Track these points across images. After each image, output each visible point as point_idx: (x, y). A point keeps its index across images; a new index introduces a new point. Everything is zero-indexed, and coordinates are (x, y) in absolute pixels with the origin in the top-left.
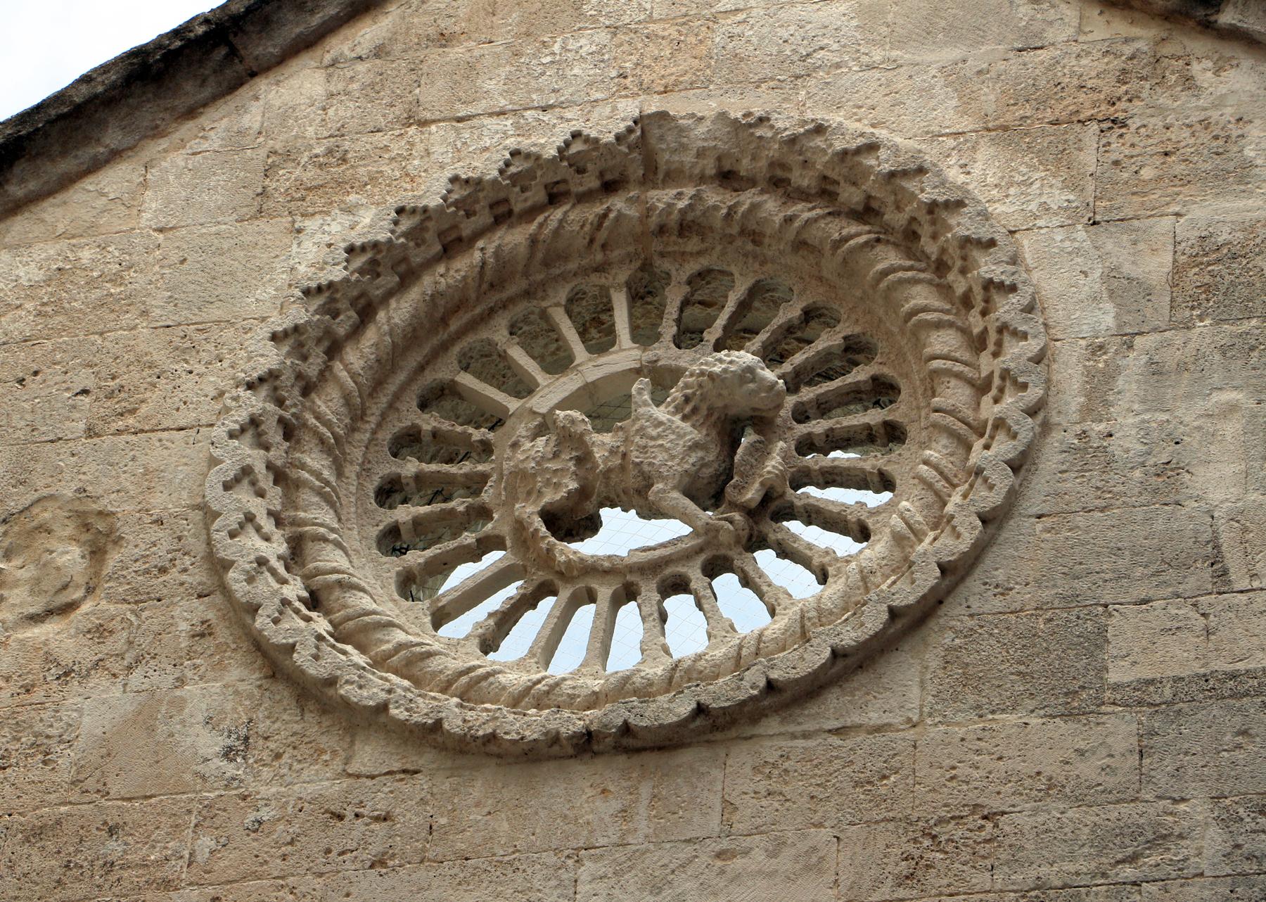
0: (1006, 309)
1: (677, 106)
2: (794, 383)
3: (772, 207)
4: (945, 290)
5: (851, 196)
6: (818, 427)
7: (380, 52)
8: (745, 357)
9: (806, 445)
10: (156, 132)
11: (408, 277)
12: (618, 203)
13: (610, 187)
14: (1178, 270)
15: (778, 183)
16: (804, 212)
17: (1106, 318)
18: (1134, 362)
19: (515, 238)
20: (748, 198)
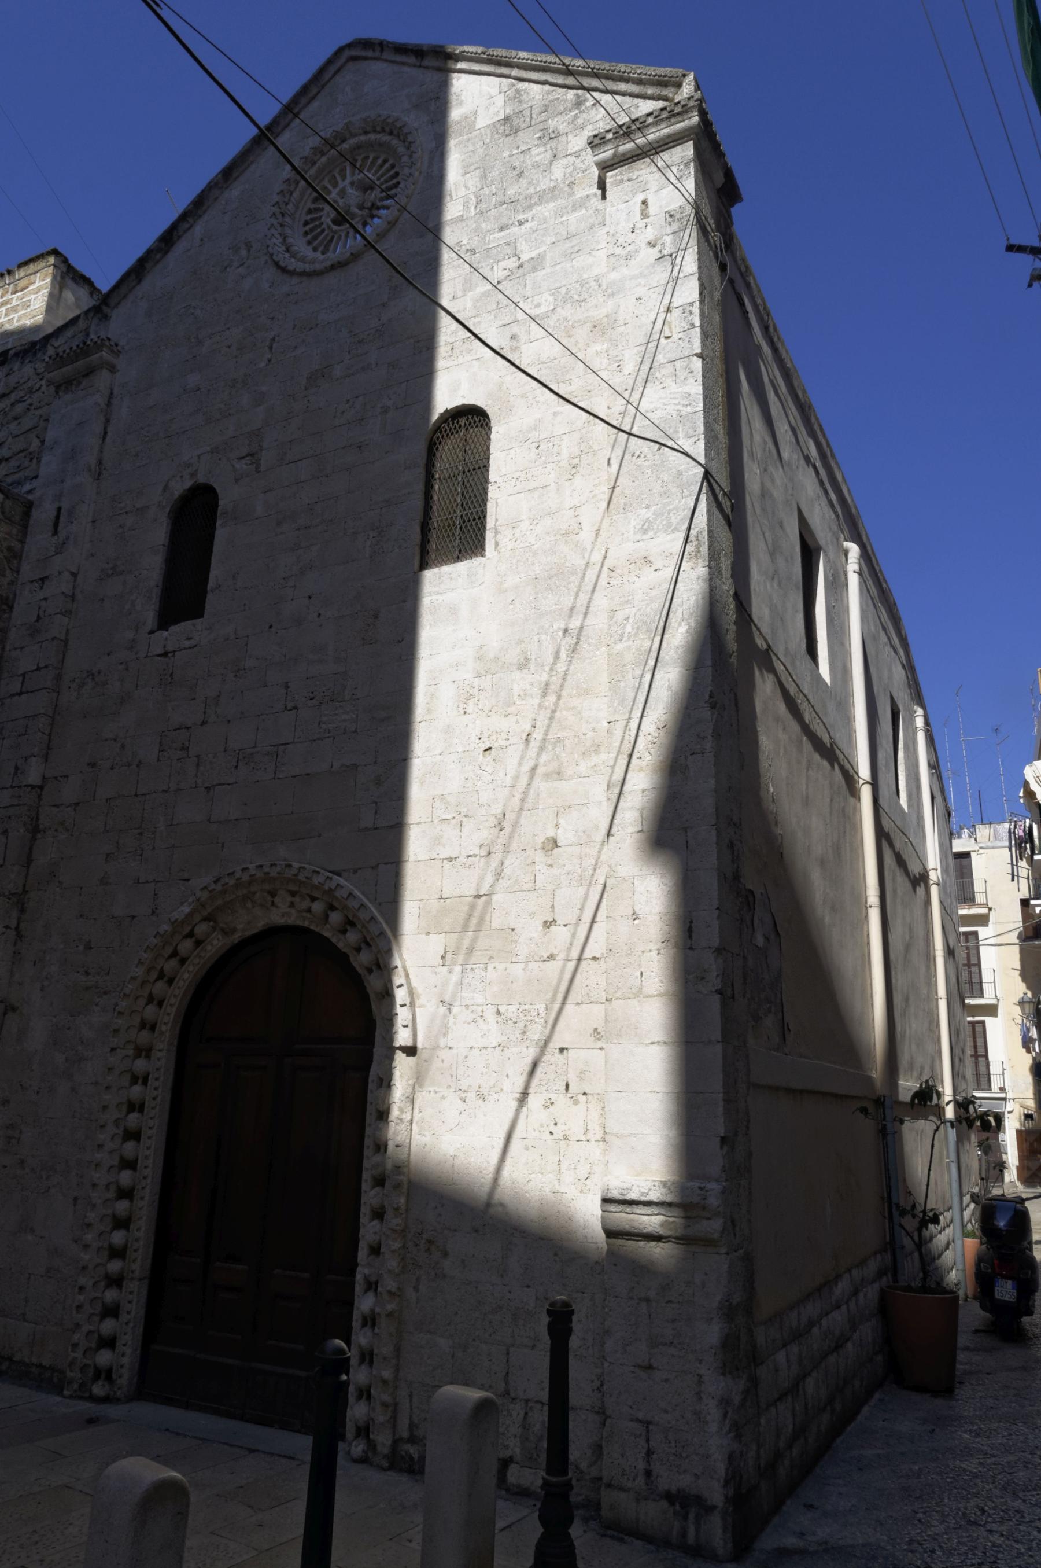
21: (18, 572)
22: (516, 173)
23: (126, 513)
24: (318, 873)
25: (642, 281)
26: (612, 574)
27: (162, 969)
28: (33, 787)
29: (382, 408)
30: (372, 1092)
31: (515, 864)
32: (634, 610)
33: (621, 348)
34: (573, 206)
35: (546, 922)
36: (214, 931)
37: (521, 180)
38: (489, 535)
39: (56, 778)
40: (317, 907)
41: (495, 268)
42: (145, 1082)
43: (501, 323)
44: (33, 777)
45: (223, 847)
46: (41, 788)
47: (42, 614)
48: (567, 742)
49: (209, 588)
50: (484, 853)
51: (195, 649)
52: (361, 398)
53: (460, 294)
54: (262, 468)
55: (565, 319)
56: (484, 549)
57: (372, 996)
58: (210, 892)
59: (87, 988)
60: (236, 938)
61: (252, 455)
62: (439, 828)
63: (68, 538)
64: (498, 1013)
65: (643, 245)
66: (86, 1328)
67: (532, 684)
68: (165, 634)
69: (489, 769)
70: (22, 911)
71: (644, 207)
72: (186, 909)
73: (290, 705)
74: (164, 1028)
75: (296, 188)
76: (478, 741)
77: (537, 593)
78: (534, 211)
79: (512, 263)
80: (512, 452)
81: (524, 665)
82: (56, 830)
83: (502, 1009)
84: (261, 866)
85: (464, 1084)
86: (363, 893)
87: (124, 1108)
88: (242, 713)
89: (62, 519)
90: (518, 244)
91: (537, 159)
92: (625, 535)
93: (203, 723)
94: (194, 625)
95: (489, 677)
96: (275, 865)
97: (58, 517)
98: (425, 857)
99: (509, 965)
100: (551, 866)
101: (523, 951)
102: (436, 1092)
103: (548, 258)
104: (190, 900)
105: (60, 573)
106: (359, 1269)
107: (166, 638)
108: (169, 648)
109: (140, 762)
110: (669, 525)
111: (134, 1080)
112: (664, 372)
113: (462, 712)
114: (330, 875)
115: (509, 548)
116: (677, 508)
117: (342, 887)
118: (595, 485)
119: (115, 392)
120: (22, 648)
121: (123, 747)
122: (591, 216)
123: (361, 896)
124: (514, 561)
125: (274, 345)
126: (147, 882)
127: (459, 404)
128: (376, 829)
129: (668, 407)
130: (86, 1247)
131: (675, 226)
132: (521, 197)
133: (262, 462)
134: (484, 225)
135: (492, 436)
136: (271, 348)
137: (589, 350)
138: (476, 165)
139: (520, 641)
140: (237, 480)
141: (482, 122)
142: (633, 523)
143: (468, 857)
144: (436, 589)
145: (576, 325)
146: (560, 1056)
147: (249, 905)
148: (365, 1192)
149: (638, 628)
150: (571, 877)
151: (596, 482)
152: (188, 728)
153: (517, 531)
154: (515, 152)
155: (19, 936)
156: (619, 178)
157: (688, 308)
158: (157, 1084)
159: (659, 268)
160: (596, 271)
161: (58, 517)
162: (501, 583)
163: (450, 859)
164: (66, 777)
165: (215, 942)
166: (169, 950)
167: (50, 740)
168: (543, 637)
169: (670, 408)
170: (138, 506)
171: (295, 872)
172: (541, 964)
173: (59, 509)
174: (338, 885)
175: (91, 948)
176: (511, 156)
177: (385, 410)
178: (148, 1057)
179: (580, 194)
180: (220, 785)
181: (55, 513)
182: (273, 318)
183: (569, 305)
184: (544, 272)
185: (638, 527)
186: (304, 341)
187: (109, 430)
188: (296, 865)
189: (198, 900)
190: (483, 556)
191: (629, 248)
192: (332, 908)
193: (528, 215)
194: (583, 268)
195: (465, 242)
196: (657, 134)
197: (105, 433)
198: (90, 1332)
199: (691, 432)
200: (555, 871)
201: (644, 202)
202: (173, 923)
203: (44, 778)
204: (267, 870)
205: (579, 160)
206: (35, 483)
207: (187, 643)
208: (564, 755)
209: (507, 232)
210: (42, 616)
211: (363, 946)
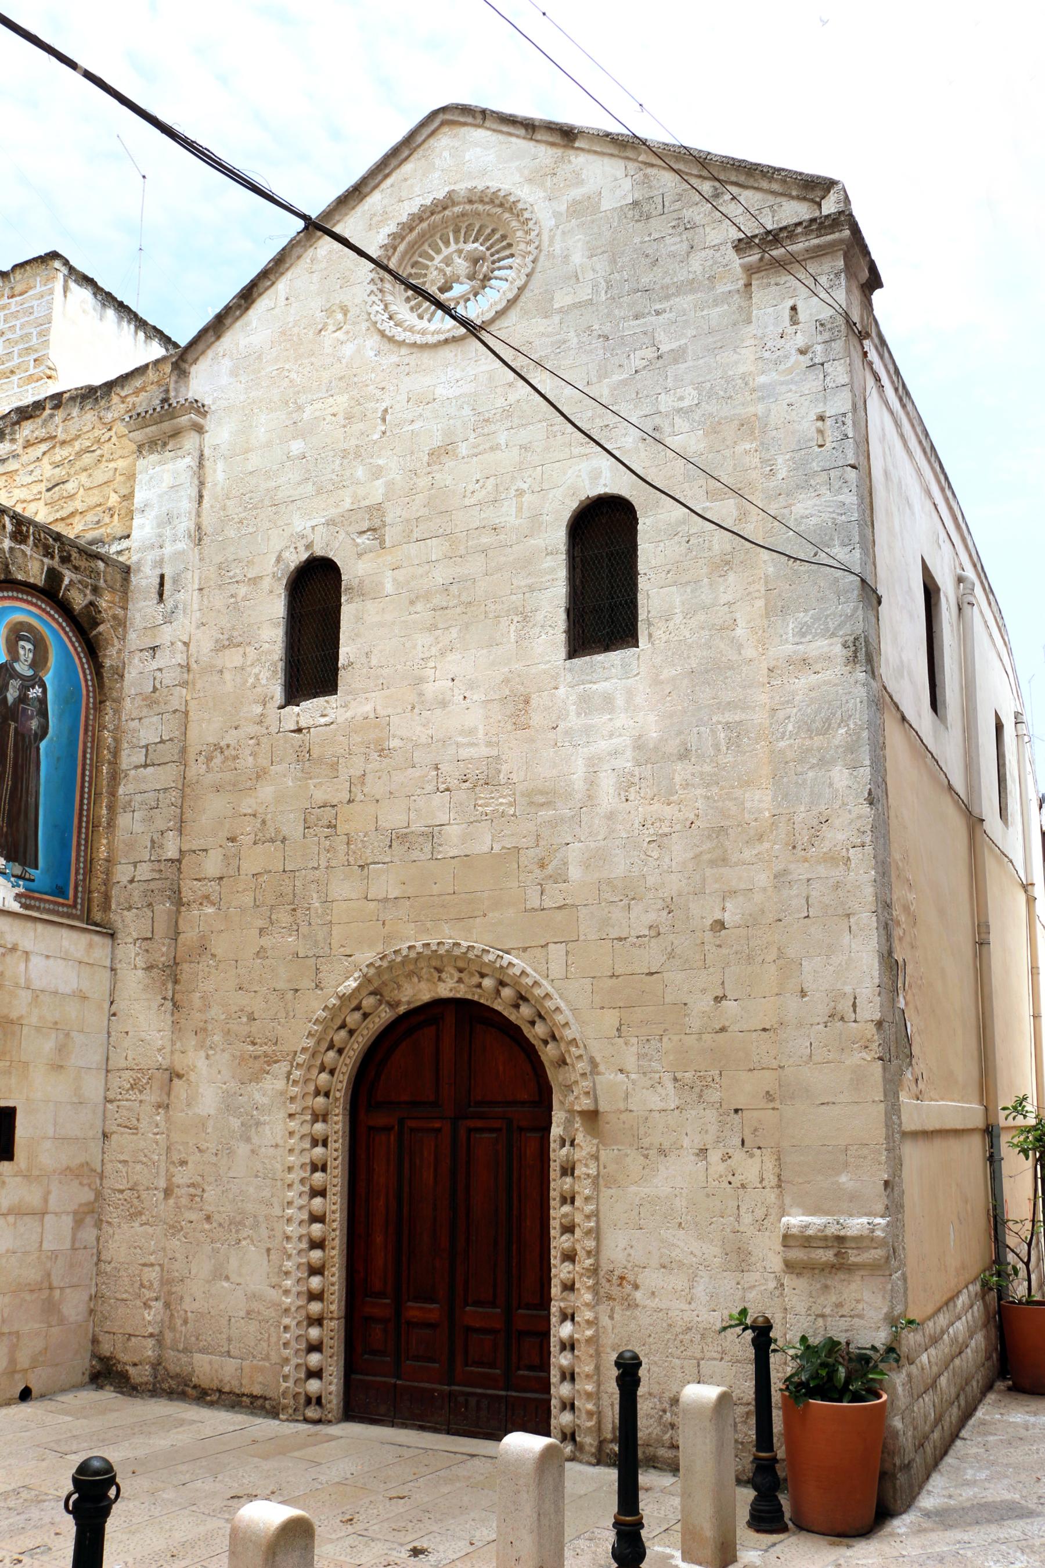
0: (531, 224)
1: (456, 187)
2: (488, 249)
3: (480, 207)
4: (519, 221)
5: (497, 202)
6: (496, 257)
7: (392, 186)
8: (476, 245)
9: (493, 262)
10: (346, 214)
11: (403, 239)
12: (447, 212)
13: (445, 209)
14: (568, 208)
15: (482, 201)
16: (487, 207)
17: (553, 222)
18: (559, 232)
19: (424, 225)
20: (475, 206)
21: (124, 639)
22: (649, 260)
23: (237, 582)
24: (488, 951)
25: (794, 388)
26: (772, 674)
27: (332, 1040)
28: (172, 861)
29: (517, 490)
30: (554, 1151)
31: (686, 944)
32: (795, 710)
33: (773, 452)
34: (714, 301)
35: (716, 998)
36: (380, 1004)
37: (655, 268)
38: (642, 627)
39: (194, 851)
40: (488, 983)
41: (632, 356)
42: (325, 1144)
43: (642, 413)
44: (172, 853)
45: (384, 924)
46: (179, 861)
47: (158, 686)
48: (730, 831)
49: (340, 665)
50: (653, 933)
51: (332, 726)
52: (492, 478)
53: (594, 380)
54: (388, 544)
55: (711, 415)
56: (637, 641)
57: (547, 1064)
58: (377, 968)
59: (256, 1058)
60: (402, 1009)
61: (374, 530)
62: (606, 910)
63: (176, 607)
64: (676, 1080)
65: (793, 352)
67: (693, 775)
68: (296, 709)
69: (655, 854)
70: (176, 982)
71: (793, 313)
72: (352, 984)
73: (442, 787)
74: (338, 1095)
75: (394, 253)
76: (641, 828)
77: (694, 686)
78: (672, 302)
79: (650, 353)
80: (662, 544)
81: (684, 755)
82: (201, 904)
83: (679, 1075)
85: (646, 1142)
86: (535, 970)
88: (391, 793)
89: (167, 587)
90: (656, 335)
91: (673, 248)
92: (784, 637)
93: (349, 801)
94: (327, 702)
95: (649, 766)
96: (443, 943)
97: (162, 584)
98: (592, 937)
99: (683, 1036)
100: (720, 946)
101: (696, 1024)
102: (619, 1150)
103: (690, 351)
104: (356, 975)
105: (172, 644)
106: (553, 1303)
107: (298, 714)
108: (303, 724)
109: (284, 838)
110: (827, 629)
112: (819, 480)
113: (624, 799)
114: (501, 953)
115: (664, 640)
116: (834, 614)
117: (514, 965)
118: (749, 583)
119: (207, 452)
120: (140, 719)
121: (264, 822)
122: (734, 313)
123: (535, 974)
124: (670, 653)
125: (388, 417)
126: (307, 957)
127: (602, 492)
128: (543, 909)
129: (823, 515)
131: (826, 336)
132: (657, 287)
133: (387, 538)
134: (616, 312)
135: (639, 527)
136: (384, 420)
137: (737, 447)
138: (603, 249)
139: (680, 733)
140: (360, 555)
141: (606, 205)
142: (791, 626)
143: (638, 937)
144: (589, 678)
145: (723, 421)
146: (735, 1116)
147: (415, 980)
148: (555, 1238)
149: (799, 727)
150: (739, 956)
151: (750, 580)
152: (333, 806)
153: (671, 624)
154: (647, 239)
155: (175, 1005)
156: (765, 281)
157: (841, 419)
158: (337, 1145)
159: (811, 376)
160: (742, 369)
161: (162, 584)
162: (657, 675)
163: (620, 939)
164: (206, 850)
165: (383, 1015)
166: (339, 1022)
167: (182, 813)
168: (703, 729)
169: (825, 516)
170: (249, 576)
171: (464, 950)
172: (713, 1035)
173: (162, 577)
174: (510, 963)
175: (255, 1019)
176: (642, 243)
177: (520, 493)
178: (325, 1121)
179: (722, 288)
180: (375, 863)
181: (158, 580)
182: (383, 389)
183: (715, 401)
184: (685, 365)
185: (796, 630)
186: (421, 415)
187: (205, 493)
188: (465, 944)
189: (365, 976)
190: (638, 647)
191: (778, 353)
192: (502, 983)
193: (665, 305)
194: (728, 365)
195: (596, 327)
196: (807, 244)
197: (201, 497)
199: (846, 541)
200: (724, 951)
201: (794, 308)
203: (181, 851)
204: (434, 948)
205: (718, 254)
206: (125, 544)
207: (323, 720)
208: (727, 843)
209: (642, 321)
210: (159, 687)
211: (537, 1019)
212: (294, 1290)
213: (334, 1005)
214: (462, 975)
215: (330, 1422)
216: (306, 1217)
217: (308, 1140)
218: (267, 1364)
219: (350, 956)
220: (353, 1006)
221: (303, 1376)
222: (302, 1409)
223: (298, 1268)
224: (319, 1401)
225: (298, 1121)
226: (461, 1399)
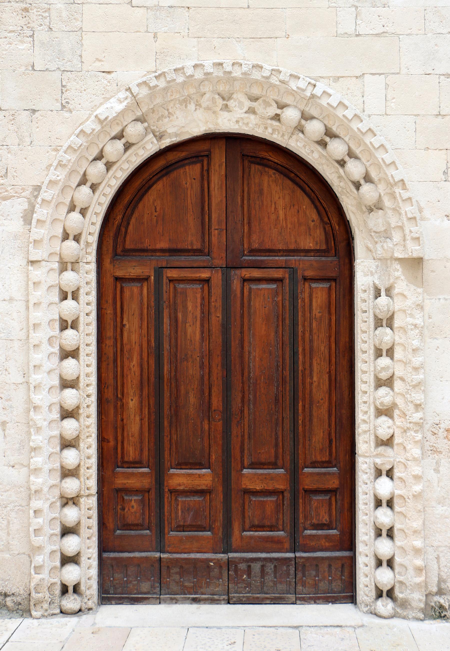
66: (49, 548)
84: (221, 64)
87: (57, 325)
111: (64, 296)
130: (36, 471)
166: (95, 152)
198: (53, 552)
202: (101, 122)
212: (46, 467)
213: (93, 130)
214: (254, 104)
215: (90, 609)
216: (56, 382)
217: (56, 292)
218: (7, 556)
219: (109, 72)
220: (113, 134)
221: (58, 563)
222: (57, 600)
223: (49, 442)
224: (76, 589)
225: (45, 270)
226: (243, 566)
